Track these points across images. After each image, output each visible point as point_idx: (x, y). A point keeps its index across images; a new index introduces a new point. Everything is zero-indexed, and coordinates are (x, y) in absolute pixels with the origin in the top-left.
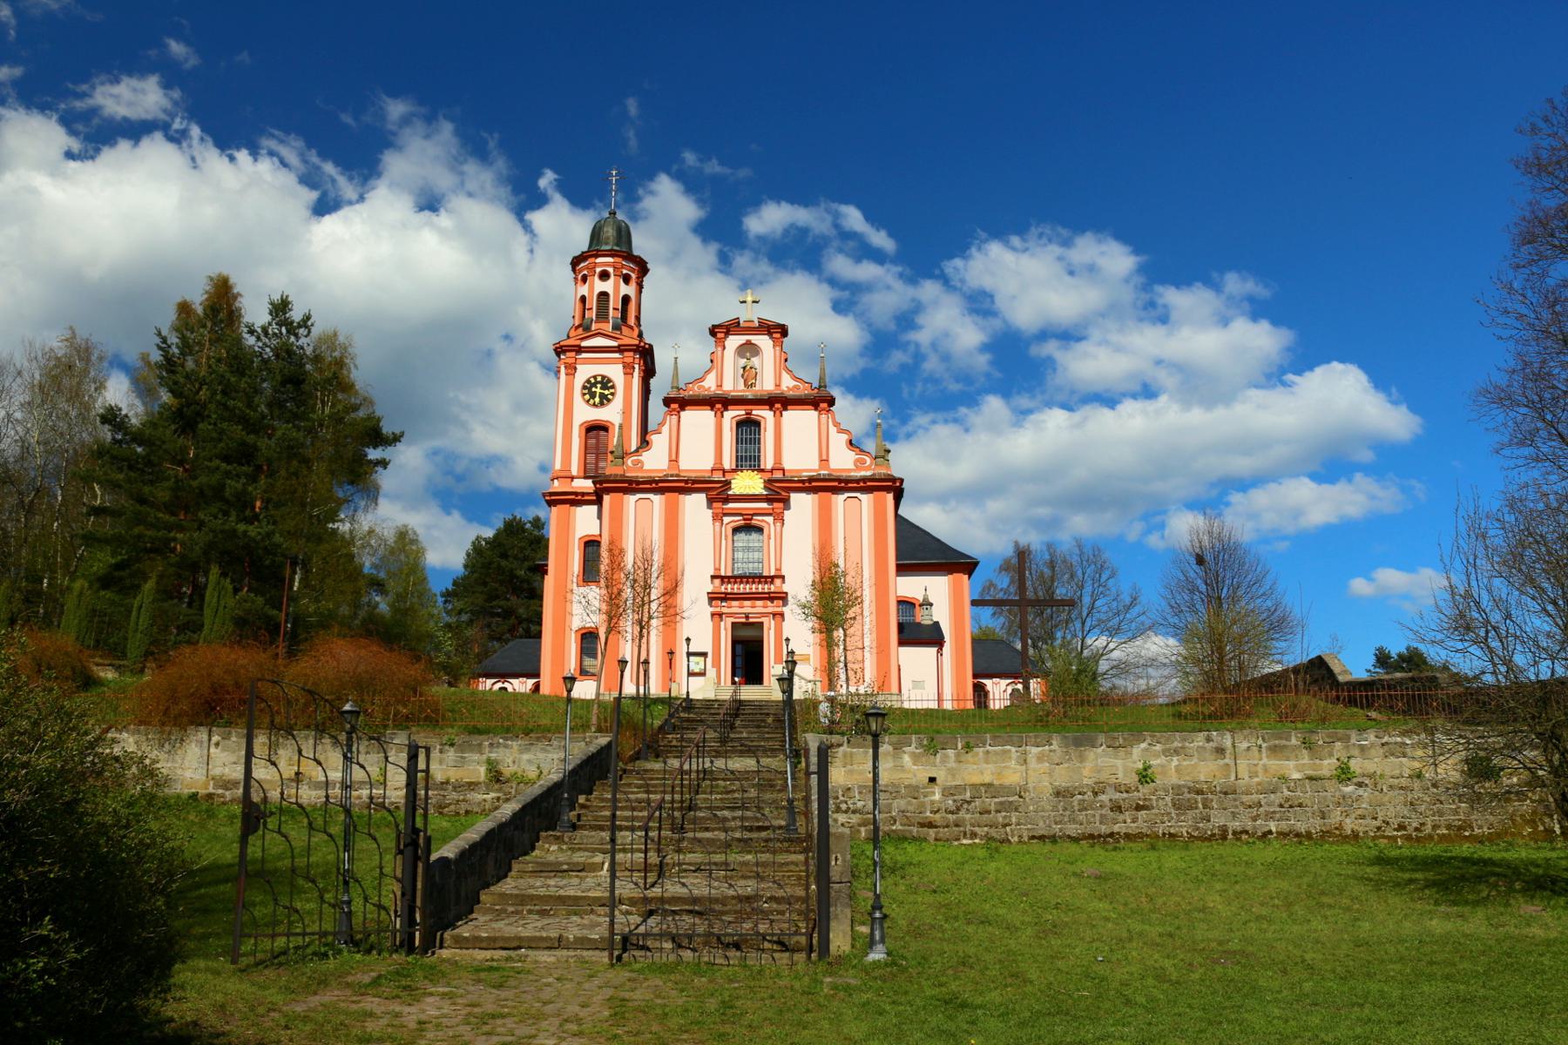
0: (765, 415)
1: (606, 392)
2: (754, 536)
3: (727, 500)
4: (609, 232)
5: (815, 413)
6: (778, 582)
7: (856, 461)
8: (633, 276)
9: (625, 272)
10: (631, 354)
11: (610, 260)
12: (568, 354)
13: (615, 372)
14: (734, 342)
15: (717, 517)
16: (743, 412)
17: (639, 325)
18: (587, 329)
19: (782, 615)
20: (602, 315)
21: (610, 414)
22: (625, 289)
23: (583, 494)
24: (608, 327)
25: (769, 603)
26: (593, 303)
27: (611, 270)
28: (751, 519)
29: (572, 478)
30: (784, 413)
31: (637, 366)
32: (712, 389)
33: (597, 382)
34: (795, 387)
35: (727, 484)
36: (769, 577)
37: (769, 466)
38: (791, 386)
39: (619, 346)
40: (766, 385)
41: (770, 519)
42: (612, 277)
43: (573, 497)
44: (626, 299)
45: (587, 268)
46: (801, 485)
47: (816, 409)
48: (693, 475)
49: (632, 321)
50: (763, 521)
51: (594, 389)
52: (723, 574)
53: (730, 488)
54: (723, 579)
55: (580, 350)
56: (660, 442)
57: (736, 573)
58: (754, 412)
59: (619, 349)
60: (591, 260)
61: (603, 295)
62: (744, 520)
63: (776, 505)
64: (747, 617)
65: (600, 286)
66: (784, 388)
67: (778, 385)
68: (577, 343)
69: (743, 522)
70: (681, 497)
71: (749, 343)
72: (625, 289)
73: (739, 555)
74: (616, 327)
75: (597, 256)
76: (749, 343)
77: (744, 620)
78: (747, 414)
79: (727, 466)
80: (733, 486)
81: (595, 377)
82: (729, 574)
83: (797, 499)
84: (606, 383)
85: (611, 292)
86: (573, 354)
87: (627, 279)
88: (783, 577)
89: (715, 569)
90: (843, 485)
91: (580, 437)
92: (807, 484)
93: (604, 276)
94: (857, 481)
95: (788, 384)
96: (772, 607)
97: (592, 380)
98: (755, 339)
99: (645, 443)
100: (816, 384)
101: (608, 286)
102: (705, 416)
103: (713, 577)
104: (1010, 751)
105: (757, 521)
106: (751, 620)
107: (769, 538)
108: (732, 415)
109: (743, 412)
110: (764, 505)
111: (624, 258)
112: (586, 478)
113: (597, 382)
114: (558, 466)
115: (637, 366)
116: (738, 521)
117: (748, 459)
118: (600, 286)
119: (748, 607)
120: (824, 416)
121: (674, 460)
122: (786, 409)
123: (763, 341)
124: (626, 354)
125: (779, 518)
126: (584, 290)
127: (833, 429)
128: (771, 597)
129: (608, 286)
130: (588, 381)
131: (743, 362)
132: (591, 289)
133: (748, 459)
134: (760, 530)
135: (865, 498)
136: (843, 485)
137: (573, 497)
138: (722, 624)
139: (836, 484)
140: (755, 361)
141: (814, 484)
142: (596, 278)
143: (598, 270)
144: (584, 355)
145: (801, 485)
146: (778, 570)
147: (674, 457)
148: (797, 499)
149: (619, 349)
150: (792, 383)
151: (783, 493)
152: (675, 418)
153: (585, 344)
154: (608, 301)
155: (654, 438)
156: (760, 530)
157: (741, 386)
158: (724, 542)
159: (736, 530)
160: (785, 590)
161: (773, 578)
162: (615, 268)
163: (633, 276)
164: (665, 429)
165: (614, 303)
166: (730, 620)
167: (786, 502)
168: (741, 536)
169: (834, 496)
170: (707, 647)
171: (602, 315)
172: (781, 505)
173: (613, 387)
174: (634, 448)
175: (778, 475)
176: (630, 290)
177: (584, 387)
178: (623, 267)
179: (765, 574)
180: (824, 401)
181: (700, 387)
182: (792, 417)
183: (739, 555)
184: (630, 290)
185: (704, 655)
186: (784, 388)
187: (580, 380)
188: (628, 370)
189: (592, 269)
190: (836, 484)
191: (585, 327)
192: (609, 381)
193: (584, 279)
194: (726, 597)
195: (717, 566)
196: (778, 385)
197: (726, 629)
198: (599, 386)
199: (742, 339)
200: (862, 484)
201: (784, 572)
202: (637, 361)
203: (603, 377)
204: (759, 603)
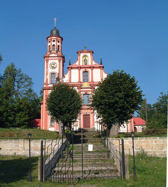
0: (89, 70)
3: (81, 88)
4: (54, 32)
9: (58, 40)
11: (55, 38)
13: (57, 61)
14: (82, 55)
17: (61, 51)
18: (51, 52)
20: (54, 49)
21: (56, 71)
22: (58, 44)
23: (51, 88)
24: (55, 52)
27: (55, 40)
35: (82, 85)
37: (90, 81)
40: (89, 63)
44: (59, 46)
45: (50, 39)
49: (60, 51)
56: (67, 76)
58: (87, 70)
61: (54, 45)
65: (53, 43)
72: (58, 44)
74: (57, 52)
79: (81, 82)
87: (59, 42)
93: (54, 41)
99: (64, 76)
101: (55, 43)
102: (77, 70)
104: (149, 141)
108: (82, 70)
112: (51, 84)
114: (45, 82)
117: (86, 79)
118: (53, 43)
120: (102, 70)
121: (70, 80)
123: (89, 55)
126: (49, 44)
129: (55, 43)
132: (51, 44)
133: (86, 79)
140: (86, 58)
143: (53, 40)
149: (58, 57)
152: (70, 71)
155: (66, 76)
164: (68, 73)
165: (56, 47)
171: (54, 49)
174: (61, 78)
175: (92, 83)
176: (59, 44)
182: (94, 70)
184: (59, 44)
189: (51, 39)
193: (50, 42)
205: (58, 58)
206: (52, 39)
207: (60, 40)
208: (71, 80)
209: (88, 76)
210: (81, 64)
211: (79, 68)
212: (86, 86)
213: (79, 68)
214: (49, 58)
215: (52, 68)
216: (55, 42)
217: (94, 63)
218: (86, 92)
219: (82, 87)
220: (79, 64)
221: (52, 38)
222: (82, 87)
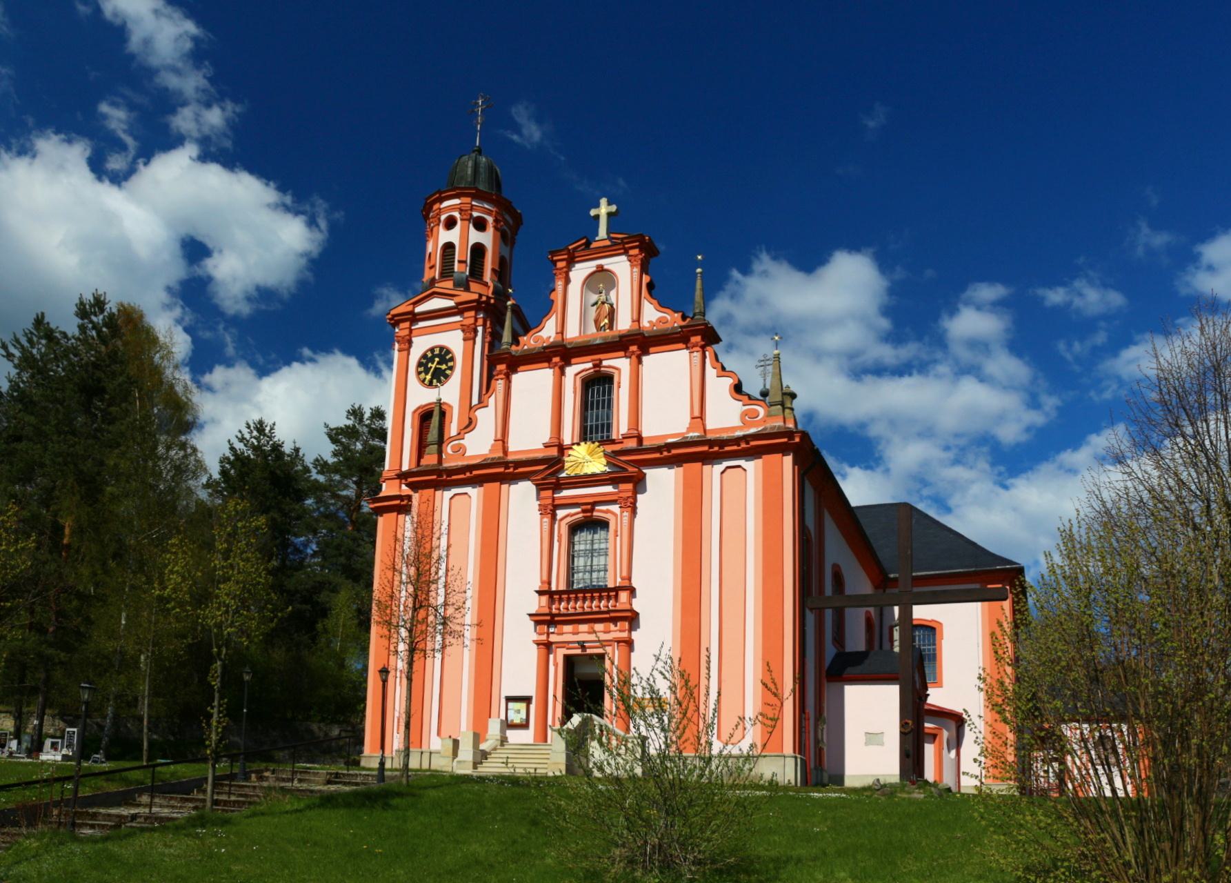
0: (620, 365)
1: (444, 367)
3: (558, 486)
5: (686, 352)
6: (623, 596)
7: (744, 414)
8: (490, 219)
9: (475, 214)
10: (472, 313)
11: (456, 201)
12: (402, 325)
13: (454, 340)
15: (550, 510)
16: (590, 365)
19: (629, 644)
22: (475, 236)
25: (612, 627)
27: (456, 214)
28: (592, 510)
30: (645, 359)
31: (480, 329)
32: (551, 340)
33: (434, 356)
34: (660, 320)
38: (654, 320)
39: (458, 304)
41: (615, 508)
42: (459, 222)
43: (397, 502)
46: (657, 455)
47: (687, 348)
48: (523, 457)
50: (608, 512)
51: (430, 365)
52: (554, 588)
53: (562, 469)
55: (414, 318)
56: (487, 418)
57: (575, 587)
59: (458, 310)
61: (449, 247)
62: (583, 511)
63: (623, 486)
64: (583, 647)
66: (645, 323)
67: (638, 320)
68: (410, 308)
69: (581, 515)
70: (505, 487)
72: (475, 236)
75: (441, 200)
77: (579, 651)
78: (595, 366)
80: (567, 465)
81: (432, 350)
82: (562, 587)
83: (652, 474)
84: (444, 355)
85: (457, 243)
86: (407, 324)
87: (480, 225)
88: (632, 591)
89: (542, 582)
90: (716, 449)
91: (413, 427)
92: (665, 453)
94: (737, 441)
95: (652, 315)
96: (617, 631)
97: (429, 355)
101: (453, 236)
103: (540, 593)
105: (600, 512)
106: (589, 651)
108: (577, 370)
110: (609, 489)
111: (474, 197)
113: (434, 356)
115: (480, 329)
116: (575, 513)
119: (583, 633)
121: (503, 439)
122: (647, 353)
124: (467, 314)
127: (711, 372)
128: (612, 618)
129: (453, 236)
130: (424, 356)
131: (594, 298)
134: (604, 525)
135: (752, 467)
136: (716, 449)
137: (397, 502)
138: (551, 657)
139: (706, 448)
141: (674, 452)
142: (441, 227)
143: (443, 217)
144: (421, 324)
145: (657, 455)
146: (630, 579)
148: (652, 474)
149: (458, 310)
151: (631, 469)
153: (419, 309)
156: (604, 525)
157: (592, 330)
159: (575, 528)
161: (612, 593)
162: (461, 211)
163: (490, 219)
165: (461, 254)
166: (561, 653)
167: (639, 483)
169: (707, 468)
172: (630, 486)
173: (452, 359)
177: (420, 364)
178: (472, 208)
179: (611, 585)
180: (695, 333)
182: (655, 362)
185: (527, 700)
186: (645, 323)
187: (416, 354)
188: (470, 334)
190: (706, 448)
192: (448, 352)
196: (638, 320)
197: (556, 665)
198: (437, 359)
200: (743, 445)
202: (480, 322)
203: (442, 348)
204: (599, 627)
205: (458, 318)
207: (489, 213)
209: (608, 404)
210: (573, 332)
211: (560, 354)
213: (560, 354)
216: (457, 229)
217: (652, 315)
220: (561, 332)
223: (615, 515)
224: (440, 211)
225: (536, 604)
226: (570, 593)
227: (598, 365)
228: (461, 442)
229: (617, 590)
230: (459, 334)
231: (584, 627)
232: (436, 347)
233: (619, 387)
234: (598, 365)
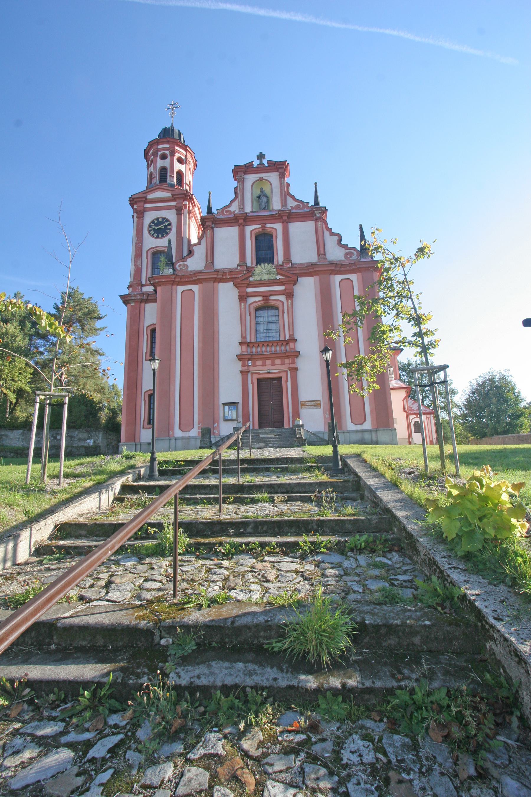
2: (271, 312)
3: (251, 285)
6: (292, 345)
15: (243, 298)
26: (157, 175)
27: (167, 152)
29: (142, 285)
34: (297, 206)
36: (285, 341)
50: (278, 300)
52: (248, 340)
54: (248, 344)
58: (268, 225)
60: (155, 147)
65: (160, 163)
71: (261, 179)
73: (262, 327)
76: (261, 179)
82: (253, 340)
89: (243, 338)
97: (156, 221)
98: (265, 175)
100: (312, 203)
107: (283, 312)
109: (259, 226)
125: (290, 295)
127: (327, 233)
129: (166, 163)
142: (158, 159)
146: (293, 335)
147: (209, 260)
150: (295, 204)
154: (167, 173)
158: (248, 318)
160: (298, 350)
166: (255, 377)
168: (264, 313)
170: (237, 397)
179: (282, 338)
181: (227, 212)
183: (262, 327)
191: (151, 188)
194: (252, 357)
195: (244, 335)
197: (252, 383)
199: (256, 177)
201: (296, 337)
205: (174, 203)
206: (158, 150)
208: (212, 262)
210: (248, 209)
212: (265, 277)
214: (147, 206)
215: (155, 235)
216: (168, 159)
218: (266, 296)
219: (251, 279)
221: (160, 147)
222: (251, 279)
223: (283, 302)
224: (158, 150)
225: (238, 350)
226: (257, 344)
227: (263, 227)
228: (185, 263)
229: (287, 342)
230: (174, 211)
231: (268, 362)
232: (160, 218)
233: (277, 238)
234: (263, 227)
